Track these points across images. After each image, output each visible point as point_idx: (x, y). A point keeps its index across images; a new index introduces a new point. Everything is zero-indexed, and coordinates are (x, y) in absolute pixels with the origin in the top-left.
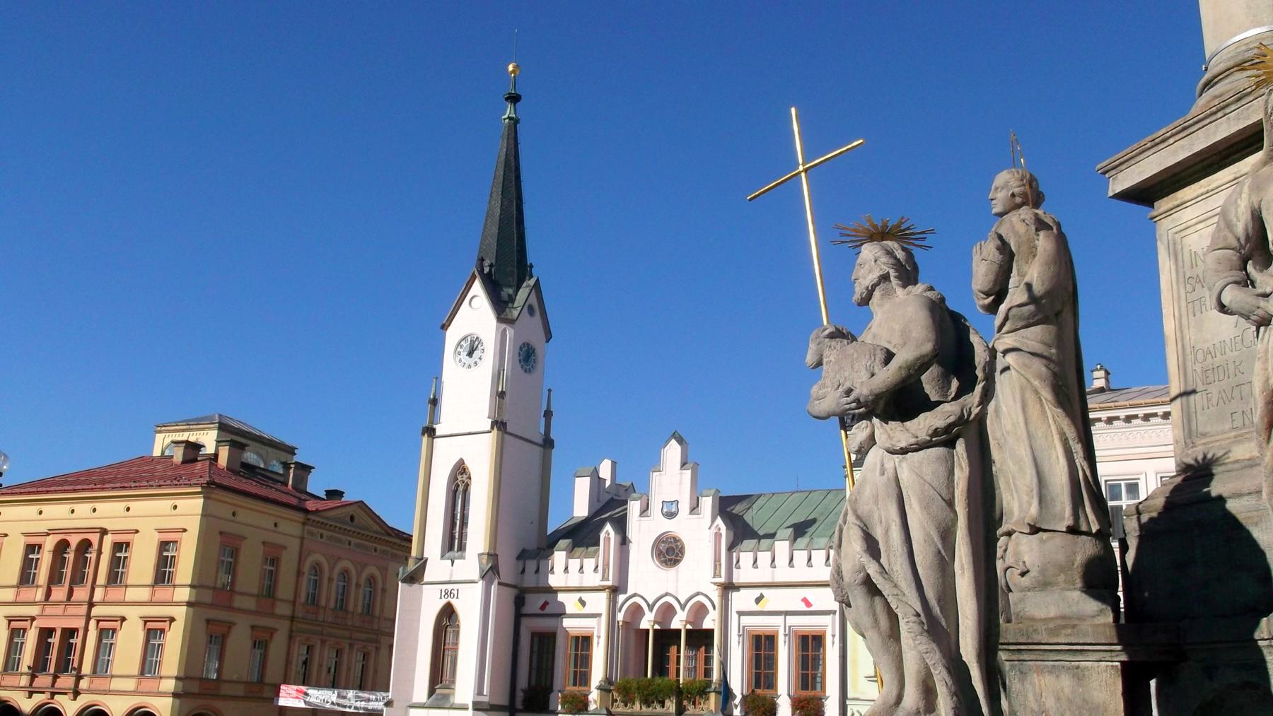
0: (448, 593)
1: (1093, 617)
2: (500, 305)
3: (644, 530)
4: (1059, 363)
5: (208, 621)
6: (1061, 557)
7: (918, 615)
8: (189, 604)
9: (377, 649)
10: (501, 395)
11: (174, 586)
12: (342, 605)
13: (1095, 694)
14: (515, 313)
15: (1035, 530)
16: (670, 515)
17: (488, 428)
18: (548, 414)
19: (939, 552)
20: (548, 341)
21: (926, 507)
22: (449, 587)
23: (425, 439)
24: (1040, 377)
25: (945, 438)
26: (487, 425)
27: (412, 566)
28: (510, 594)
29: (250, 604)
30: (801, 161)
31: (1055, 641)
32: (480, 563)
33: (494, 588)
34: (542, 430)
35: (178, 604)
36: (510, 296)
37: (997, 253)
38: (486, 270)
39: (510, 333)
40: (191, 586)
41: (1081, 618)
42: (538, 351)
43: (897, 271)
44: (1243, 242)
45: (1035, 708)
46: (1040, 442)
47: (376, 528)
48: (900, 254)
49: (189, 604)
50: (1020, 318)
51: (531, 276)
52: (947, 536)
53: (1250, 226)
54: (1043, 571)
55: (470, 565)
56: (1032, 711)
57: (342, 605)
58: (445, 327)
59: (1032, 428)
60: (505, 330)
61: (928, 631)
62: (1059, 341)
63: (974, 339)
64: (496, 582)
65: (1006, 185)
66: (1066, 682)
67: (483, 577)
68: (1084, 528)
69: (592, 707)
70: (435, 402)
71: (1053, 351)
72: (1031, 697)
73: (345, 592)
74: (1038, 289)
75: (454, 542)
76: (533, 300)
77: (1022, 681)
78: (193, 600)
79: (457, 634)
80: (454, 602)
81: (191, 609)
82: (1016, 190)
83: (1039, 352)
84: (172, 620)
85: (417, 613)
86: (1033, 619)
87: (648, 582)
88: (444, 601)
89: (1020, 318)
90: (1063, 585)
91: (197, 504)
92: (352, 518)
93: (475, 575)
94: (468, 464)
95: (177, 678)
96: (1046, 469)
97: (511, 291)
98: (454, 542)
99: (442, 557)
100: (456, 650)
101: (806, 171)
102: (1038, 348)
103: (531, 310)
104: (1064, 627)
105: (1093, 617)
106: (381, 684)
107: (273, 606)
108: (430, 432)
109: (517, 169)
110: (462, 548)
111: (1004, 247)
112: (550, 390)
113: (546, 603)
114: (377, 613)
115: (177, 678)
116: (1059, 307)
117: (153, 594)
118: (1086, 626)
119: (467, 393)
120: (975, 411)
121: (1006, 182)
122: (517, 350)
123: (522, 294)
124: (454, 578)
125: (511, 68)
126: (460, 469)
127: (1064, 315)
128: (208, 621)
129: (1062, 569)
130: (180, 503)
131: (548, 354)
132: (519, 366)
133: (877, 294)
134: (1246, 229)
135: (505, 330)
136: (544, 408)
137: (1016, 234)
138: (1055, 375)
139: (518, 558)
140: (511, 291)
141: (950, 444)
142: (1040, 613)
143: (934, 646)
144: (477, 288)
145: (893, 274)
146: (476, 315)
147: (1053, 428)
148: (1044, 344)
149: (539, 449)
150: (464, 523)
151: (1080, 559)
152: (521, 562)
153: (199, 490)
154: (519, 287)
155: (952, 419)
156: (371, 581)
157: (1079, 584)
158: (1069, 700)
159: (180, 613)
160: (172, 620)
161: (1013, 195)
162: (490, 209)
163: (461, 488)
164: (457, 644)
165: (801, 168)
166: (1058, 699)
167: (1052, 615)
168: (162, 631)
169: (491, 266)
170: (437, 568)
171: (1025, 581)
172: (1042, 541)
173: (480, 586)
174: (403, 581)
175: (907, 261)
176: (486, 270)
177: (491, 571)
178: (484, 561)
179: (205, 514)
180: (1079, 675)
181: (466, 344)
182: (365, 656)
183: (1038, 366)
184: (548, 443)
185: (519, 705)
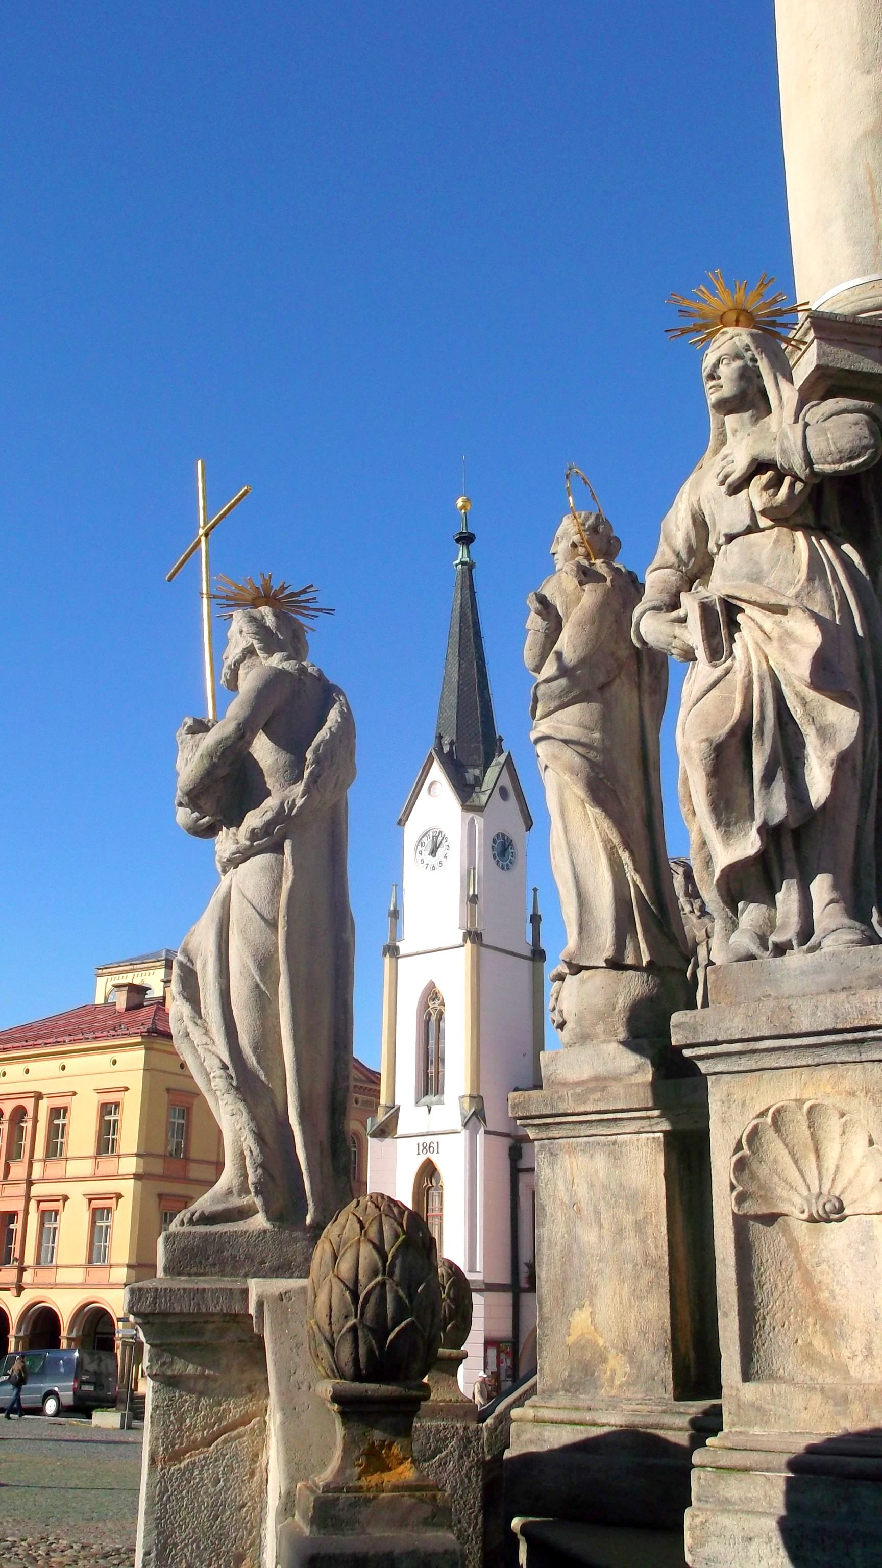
0: (427, 1148)
1: (631, 1075)
2: (465, 790)
4: (605, 751)
5: (160, 1196)
6: (599, 1001)
7: (225, 1067)
8: (137, 1177)
10: (473, 900)
11: (119, 1156)
13: (634, 1176)
14: (484, 798)
15: (576, 969)
17: (461, 941)
18: (536, 919)
19: (257, 986)
20: (528, 829)
21: (243, 931)
22: (428, 1139)
23: (387, 960)
24: (572, 771)
25: (269, 840)
26: (458, 937)
27: (381, 1117)
28: (504, 1144)
30: (202, 524)
31: (582, 1109)
32: (462, 1108)
33: (480, 1137)
35: (124, 1177)
36: (476, 778)
37: (539, 619)
38: (446, 749)
39: (479, 822)
40: (137, 1155)
41: (617, 1078)
42: (517, 842)
43: (260, 640)
44: (684, 556)
45: (566, 1199)
46: (583, 856)
48: (270, 621)
49: (137, 1177)
50: (551, 698)
51: (501, 752)
52: (265, 964)
53: (693, 535)
54: (580, 1020)
55: (451, 1109)
56: (562, 1203)
58: (401, 823)
59: (573, 839)
60: (472, 819)
61: (237, 1089)
62: (606, 721)
63: (333, 716)
64: (482, 1130)
65: (566, 534)
66: (601, 1162)
67: (465, 1125)
68: (630, 960)
70: (396, 914)
71: (597, 735)
72: (561, 1185)
74: (570, 657)
75: (430, 1084)
76: (506, 780)
77: (552, 1165)
78: (141, 1171)
79: (441, 1196)
80: (434, 1158)
81: (140, 1183)
82: (576, 538)
83: (575, 738)
84: (119, 1196)
86: (565, 1084)
88: (422, 1158)
89: (551, 698)
90: (603, 1037)
91: (138, 1056)
93: (457, 1124)
94: (440, 987)
95: (129, 1266)
96: (590, 887)
97: (477, 772)
98: (430, 1084)
99: (417, 1103)
100: (440, 1217)
101: (206, 535)
102: (572, 731)
103: (504, 793)
104: (592, 1090)
105: (631, 1075)
107: (185, 1169)
108: (392, 951)
109: (476, 623)
110: (439, 1090)
111: (546, 607)
112: (535, 890)
115: (129, 1266)
116: (602, 679)
117: (96, 1167)
118: (616, 1088)
120: (299, 802)
121: (568, 530)
122: (490, 843)
123: (492, 773)
124: (432, 1129)
125: (460, 503)
126: (431, 994)
127: (615, 687)
128: (160, 1196)
129: (603, 1016)
130: (120, 1056)
132: (493, 862)
133: (241, 672)
134: (688, 539)
135: (472, 822)
136: (530, 912)
137: (563, 592)
138: (592, 764)
140: (477, 772)
141: (277, 849)
142: (572, 1076)
143: (241, 1106)
144: (437, 772)
145: (257, 645)
146: (437, 804)
147: (596, 833)
148: (586, 727)
149: (527, 964)
150: (440, 1060)
151: (623, 1001)
153: (139, 1039)
154: (486, 767)
155: (269, 815)
157: (622, 1035)
158: (605, 1187)
159: (127, 1187)
160: (119, 1196)
161: (574, 545)
162: (446, 675)
164: (441, 1210)
165: (201, 532)
166: (592, 1186)
167: (585, 1076)
168: (109, 1210)
169: (451, 743)
170: (412, 1116)
171: (565, 1035)
172: (583, 982)
173: (464, 1134)
174: (374, 1135)
175: (278, 628)
176: (446, 749)
177: (477, 1115)
178: (466, 1106)
179: (149, 1069)
180: (615, 1153)
181: (428, 842)
183: (570, 756)
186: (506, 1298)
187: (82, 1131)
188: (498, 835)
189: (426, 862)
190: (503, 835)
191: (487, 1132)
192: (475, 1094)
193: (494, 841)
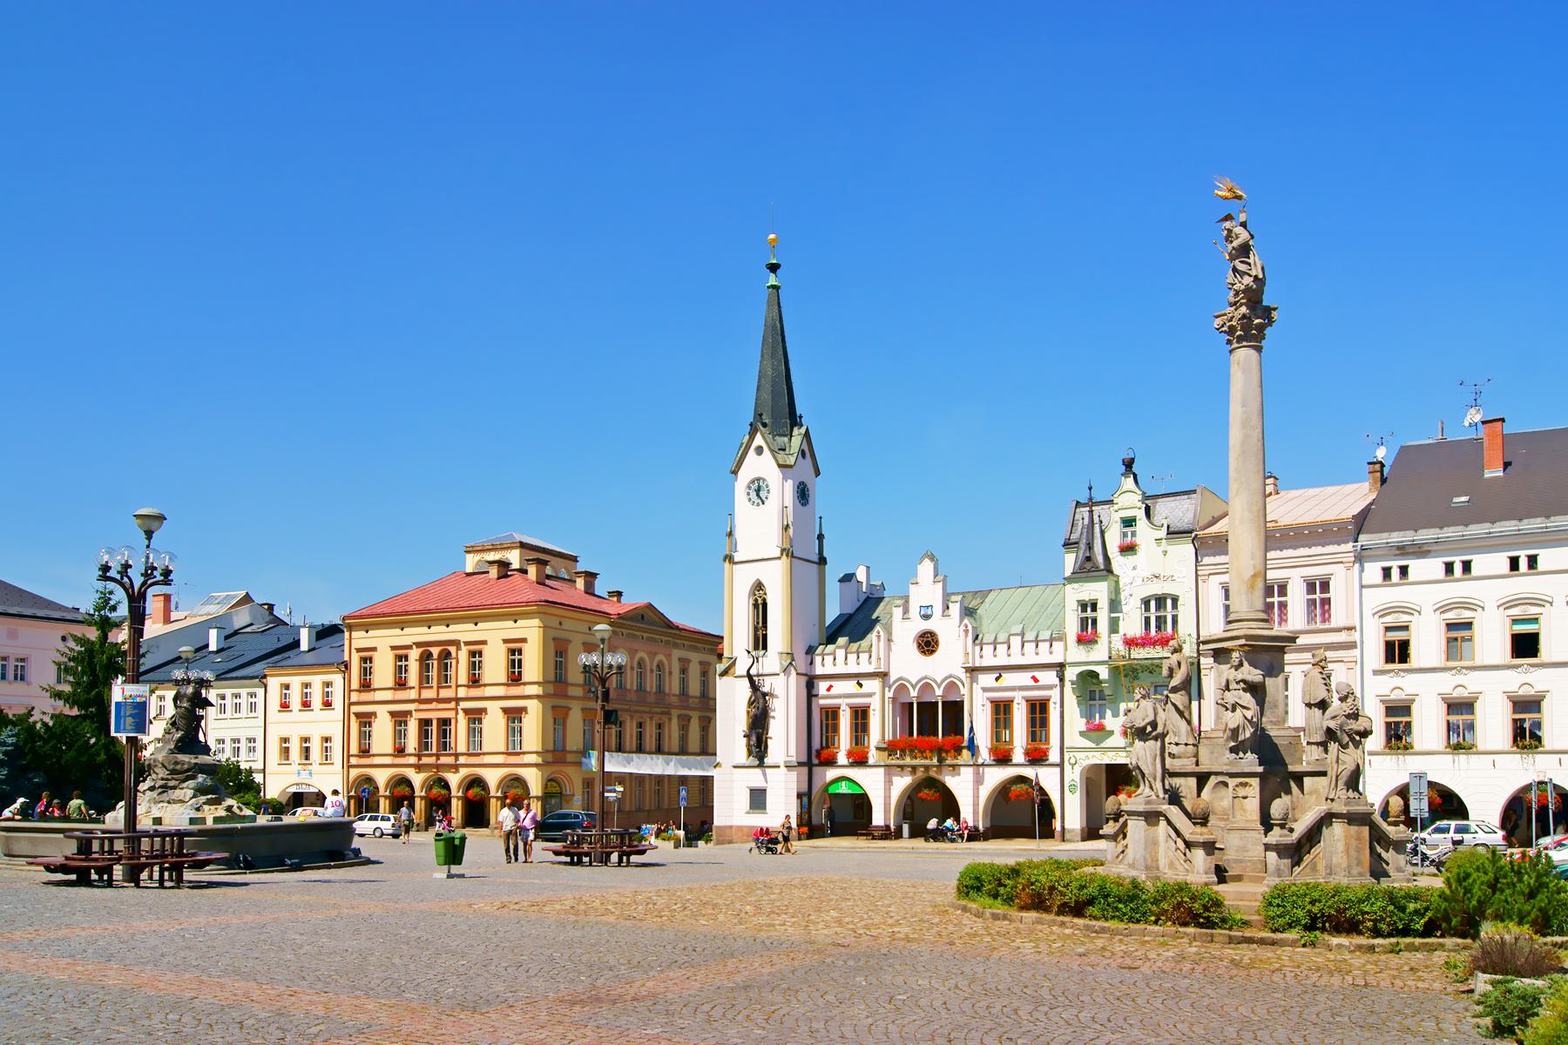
3: (905, 631)
12: (641, 688)
16: (926, 617)
18: (821, 537)
28: (804, 680)
29: (578, 692)
57: (641, 688)
69: (871, 761)
73: (641, 675)
75: (760, 641)
85: (732, 700)
87: (909, 666)
98: (760, 641)
103: (804, 456)
108: (729, 558)
110: (765, 647)
119: (760, 528)
126: (759, 586)
131: (818, 489)
146: (760, 465)
182: (659, 726)
184: (822, 561)
185: (815, 761)
186: (805, 769)
187: (495, 667)
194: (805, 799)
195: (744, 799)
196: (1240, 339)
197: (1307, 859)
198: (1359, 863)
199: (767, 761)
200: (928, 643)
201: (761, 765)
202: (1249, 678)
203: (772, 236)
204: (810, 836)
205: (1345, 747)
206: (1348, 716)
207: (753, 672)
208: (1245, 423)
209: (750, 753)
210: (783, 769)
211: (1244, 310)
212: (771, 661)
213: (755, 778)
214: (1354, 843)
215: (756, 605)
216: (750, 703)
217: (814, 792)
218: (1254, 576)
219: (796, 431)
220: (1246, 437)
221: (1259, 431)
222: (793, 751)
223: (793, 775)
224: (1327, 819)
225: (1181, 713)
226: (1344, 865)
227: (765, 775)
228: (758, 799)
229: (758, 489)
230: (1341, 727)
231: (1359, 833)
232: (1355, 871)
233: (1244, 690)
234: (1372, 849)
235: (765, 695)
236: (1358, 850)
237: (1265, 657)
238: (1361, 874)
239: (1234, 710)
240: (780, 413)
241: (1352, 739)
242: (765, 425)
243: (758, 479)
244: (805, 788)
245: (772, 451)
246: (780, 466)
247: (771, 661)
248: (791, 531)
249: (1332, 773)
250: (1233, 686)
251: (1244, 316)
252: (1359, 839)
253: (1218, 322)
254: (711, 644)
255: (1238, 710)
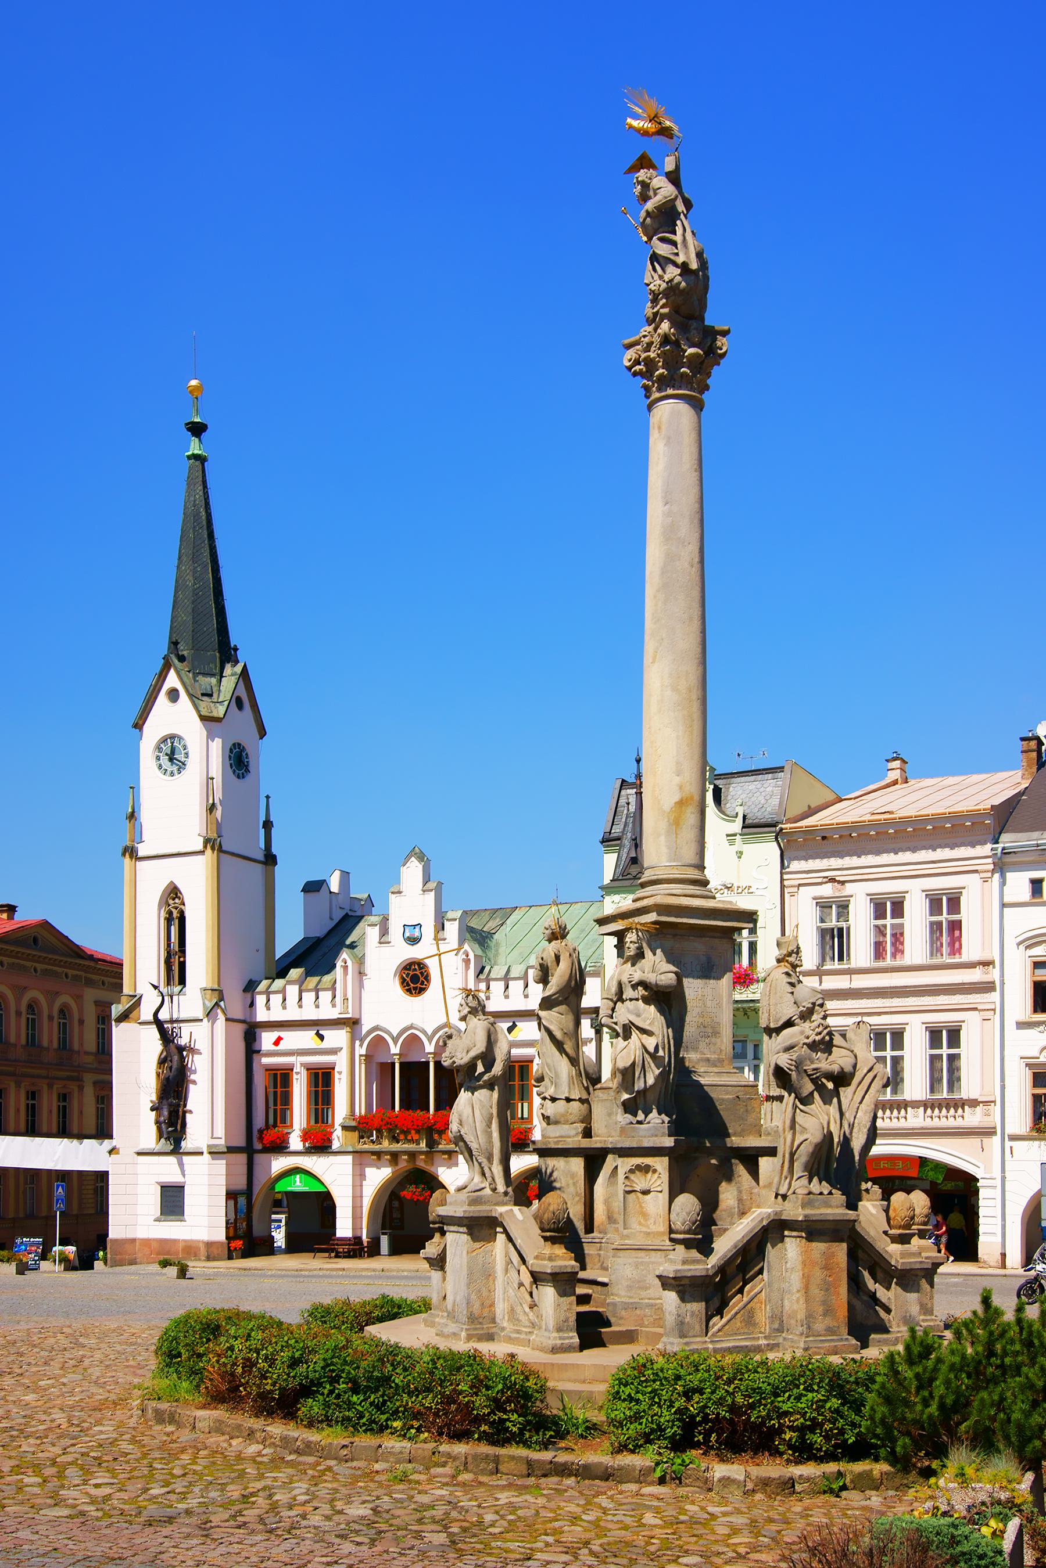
3: (380, 956)
9: (81, 1088)
12: (33, 1041)
16: (413, 941)
18: (268, 825)
20: (261, 738)
23: (127, 860)
28: (239, 1029)
34: (262, 845)
42: (249, 749)
47: (54, 941)
51: (237, 662)
57: (33, 1041)
58: (139, 726)
69: (336, 1145)
73: (32, 1025)
76: (242, 693)
87: (388, 1010)
92: (35, 940)
106: (103, 1131)
110: (182, 981)
112: (268, 797)
113: (280, 1039)
114: (76, 1047)
119: (175, 808)
126: (173, 892)
131: (266, 757)
132: (230, 771)
136: (263, 818)
139: (245, 990)
146: (175, 716)
149: (259, 867)
152: (249, 995)
156: (63, 1012)
163: (175, 914)
182: (64, 1097)
184: (270, 859)
185: (258, 1146)
186: (243, 1158)
188: (234, 745)
189: (164, 767)
190: (239, 744)
191: (227, 1020)
192: (216, 987)
193: (231, 751)
194: (242, 1200)
195: (153, 1201)
196: (663, 383)
197: (736, 1303)
198: (828, 1312)
199: (186, 1145)
200: (414, 978)
201: (176, 1151)
202: (651, 978)
203: (194, 383)
204: (246, 1254)
205: (806, 1101)
206: (813, 1046)
207: (163, 1015)
208: (669, 533)
209: (160, 1135)
210: (206, 1155)
211: (665, 326)
212: (191, 1002)
213: (167, 1169)
214: (818, 1274)
215: (169, 920)
216: (162, 1062)
217: (256, 1189)
218: (681, 803)
219: (228, 669)
220: (670, 558)
221: (693, 548)
222: (220, 1130)
223: (221, 1165)
224: (774, 1230)
225: (559, 1045)
226: (801, 1315)
227: (181, 1165)
228: (172, 1200)
229: (172, 753)
230: (798, 1064)
231: (828, 1256)
232: (819, 1326)
233: (646, 1000)
234: (855, 1282)
235: (181, 1049)
236: (827, 1287)
237: (699, 946)
238: (830, 1331)
239: (627, 1036)
240: (204, 641)
241: (820, 1088)
242: (182, 659)
243: (172, 737)
244: (241, 1183)
245: (191, 696)
246: (203, 718)
247: (191, 1002)
248: (218, 813)
249: (783, 1150)
250: (629, 993)
251: (666, 340)
252: (828, 1267)
253: (631, 354)
254: (108, 973)
255: (635, 1035)
